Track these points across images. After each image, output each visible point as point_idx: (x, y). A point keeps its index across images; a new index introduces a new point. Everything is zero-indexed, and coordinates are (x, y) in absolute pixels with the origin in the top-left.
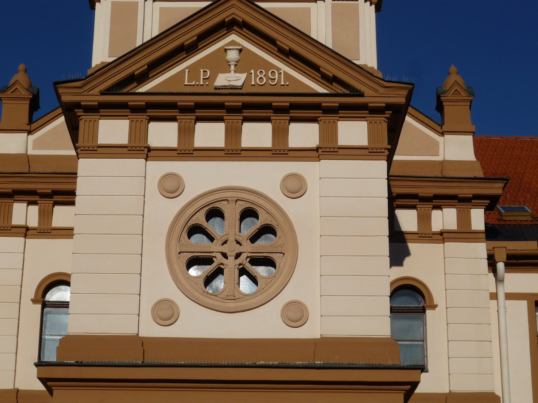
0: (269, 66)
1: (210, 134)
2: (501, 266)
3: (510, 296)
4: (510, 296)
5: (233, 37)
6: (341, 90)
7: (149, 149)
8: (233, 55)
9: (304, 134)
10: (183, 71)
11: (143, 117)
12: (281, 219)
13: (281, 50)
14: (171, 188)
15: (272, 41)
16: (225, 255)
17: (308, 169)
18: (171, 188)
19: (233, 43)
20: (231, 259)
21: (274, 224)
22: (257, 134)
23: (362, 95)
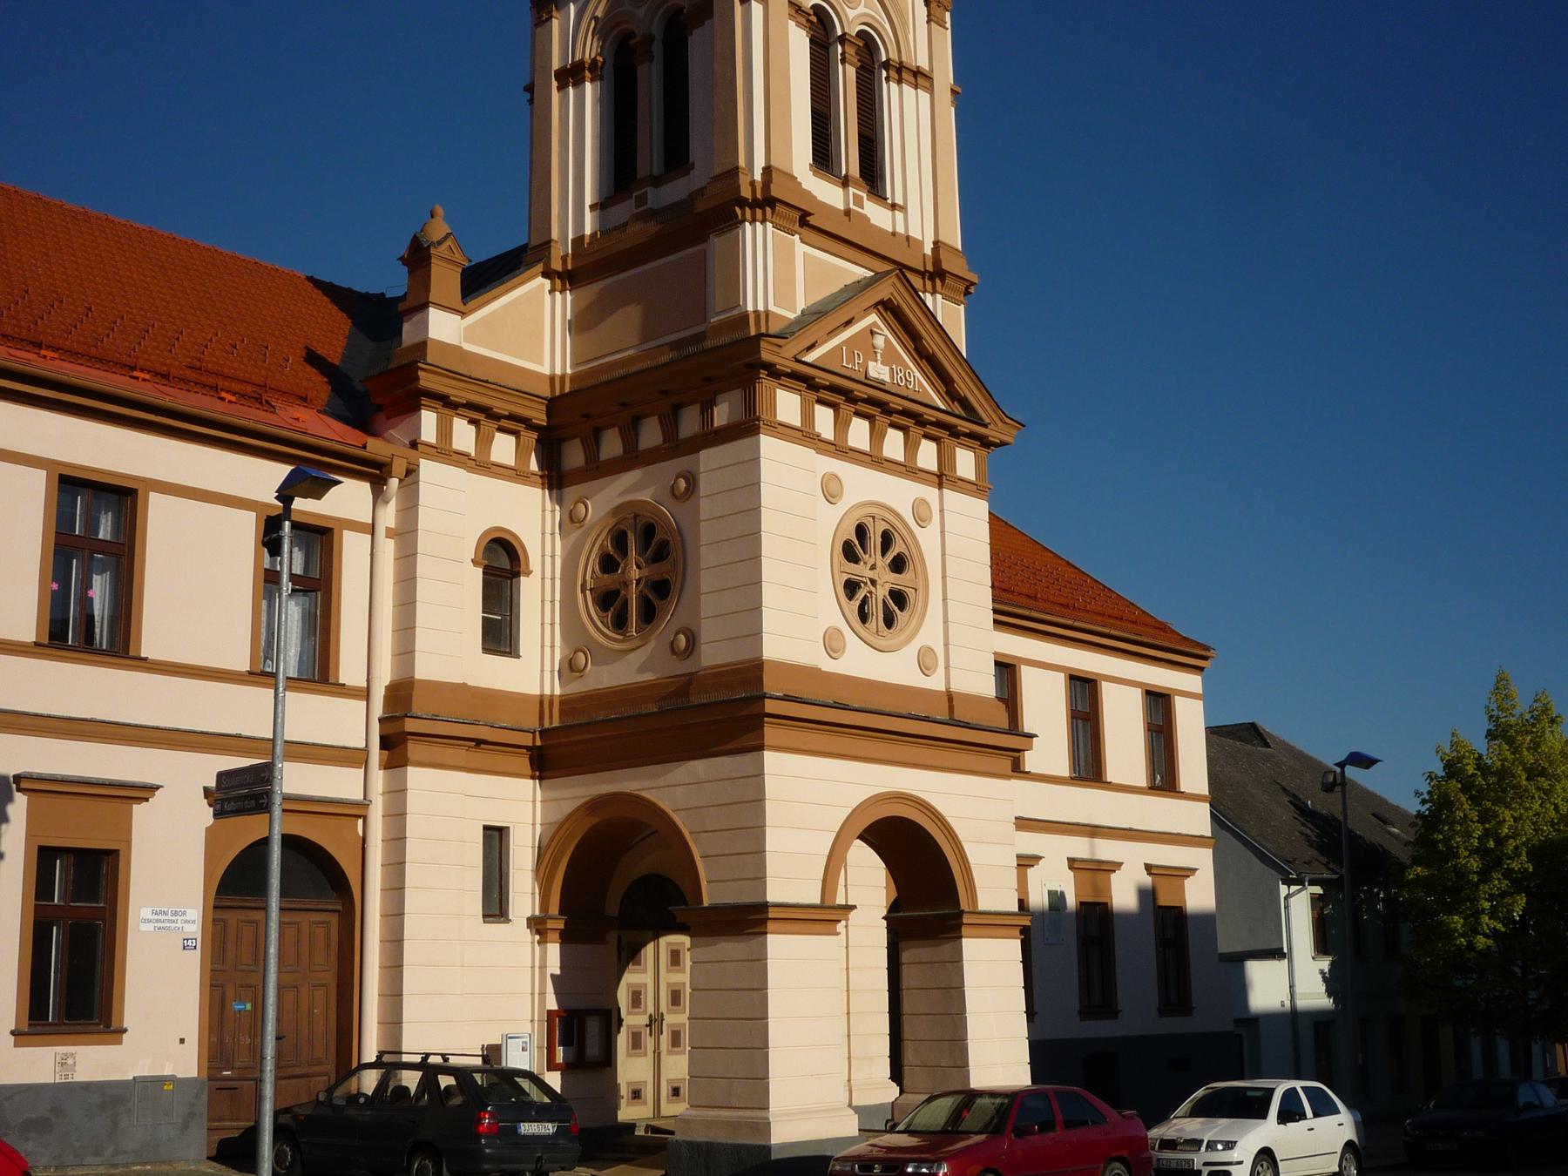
10: (839, 347)
16: (873, 582)
18: (831, 490)
23: (986, 426)
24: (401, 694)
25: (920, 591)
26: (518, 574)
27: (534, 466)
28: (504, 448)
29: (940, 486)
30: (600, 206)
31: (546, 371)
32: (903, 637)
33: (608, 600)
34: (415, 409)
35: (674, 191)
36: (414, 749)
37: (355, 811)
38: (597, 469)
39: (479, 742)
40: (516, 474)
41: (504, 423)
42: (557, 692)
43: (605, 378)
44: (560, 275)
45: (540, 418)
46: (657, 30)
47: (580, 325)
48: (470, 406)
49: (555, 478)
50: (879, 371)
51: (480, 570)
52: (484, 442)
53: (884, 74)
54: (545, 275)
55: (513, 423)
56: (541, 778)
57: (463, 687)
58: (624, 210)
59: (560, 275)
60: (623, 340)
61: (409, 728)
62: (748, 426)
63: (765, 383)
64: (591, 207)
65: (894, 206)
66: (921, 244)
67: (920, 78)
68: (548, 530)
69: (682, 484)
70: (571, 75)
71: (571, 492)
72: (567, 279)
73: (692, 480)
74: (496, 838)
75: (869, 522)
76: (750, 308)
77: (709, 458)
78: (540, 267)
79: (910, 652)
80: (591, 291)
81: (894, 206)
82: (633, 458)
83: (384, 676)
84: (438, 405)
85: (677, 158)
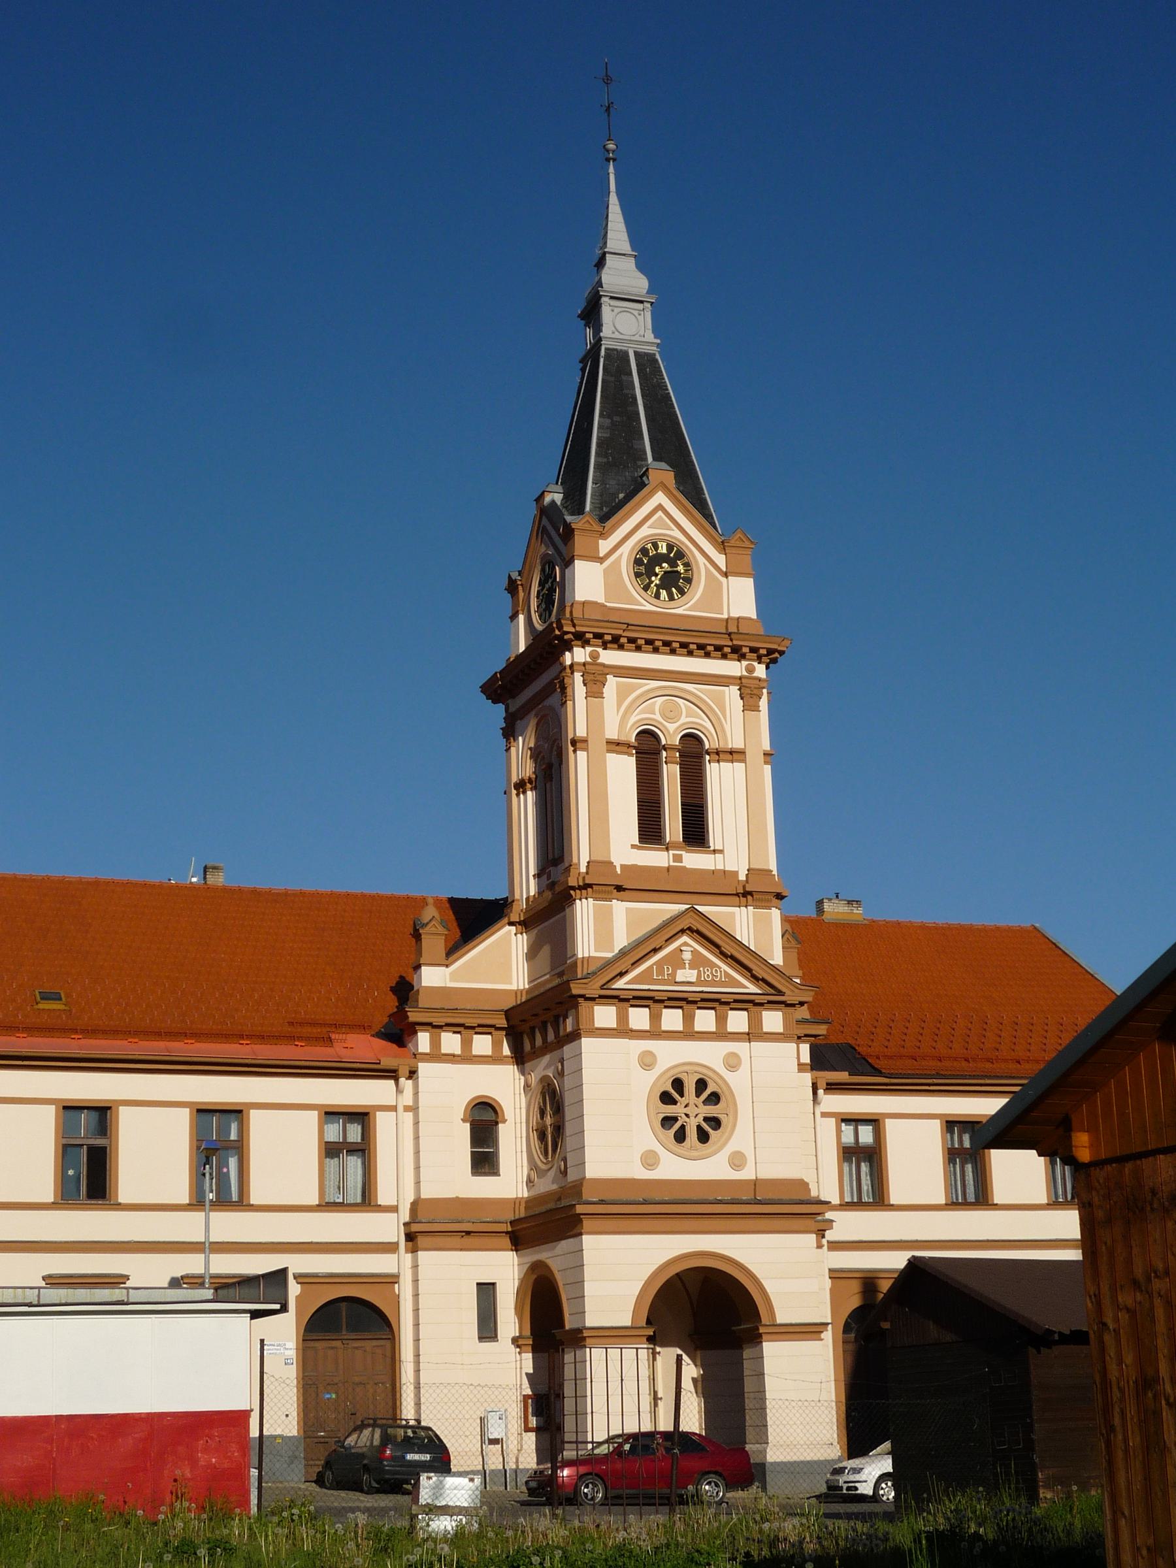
0: (713, 965)
1: (672, 1019)
2: (821, 1092)
3: (824, 1115)
4: (824, 1115)
5: (685, 938)
6: (773, 991)
7: (632, 1031)
8: (687, 956)
9: (738, 1021)
10: (651, 967)
11: (626, 1004)
12: (724, 1088)
13: (722, 953)
14: (647, 1061)
15: (718, 946)
16: (687, 1115)
17: (741, 1048)
18: (647, 1061)
19: (686, 944)
20: (692, 1118)
21: (719, 1091)
22: (705, 1020)
23: (783, 994)
24: (415, 1206)
25: (731, 1117)
26: (497, 1123)
27: (506, 1051)
28: (482, 1044)
30: (538, 876)
31: (514, 987)
32: (715, 1148)
33: (542, 1136)
34: (415, 1033)
36: (421, 1240)
37: (392, 1280)
38: (537, 1053)
39: (468, 1233)
40: (494, 1059)
41: (478, 1030)
42: (526, 1195)
43: (542, 990)
44: (520, 923)
45: (503, 1023)
48: (447, 1025)
49: (520, 1058)
50: (686, 975)
51: (468, 1125)
52: (467, 1044)
53: (708, 757)
54: (511, 924)
55: (484, 1029)
56: (517, 1250)
57: (457, 1200)
59: (520, 923)
61: (427, 1227)
63: (584, 1005)
65: (714, 851)
66: (736, 873)
67: (735, 755)
68: (517, 1092)
70: (521, 786)
71: (528, 1065)
74: (486, 1290)
75: (684, 1077)
76: (580, 956)
78: (506, 920)
79: (722, 1157)
80: (535, 931)
81: (714, 851)
83: (411, 1198)
84: (429, 1028)
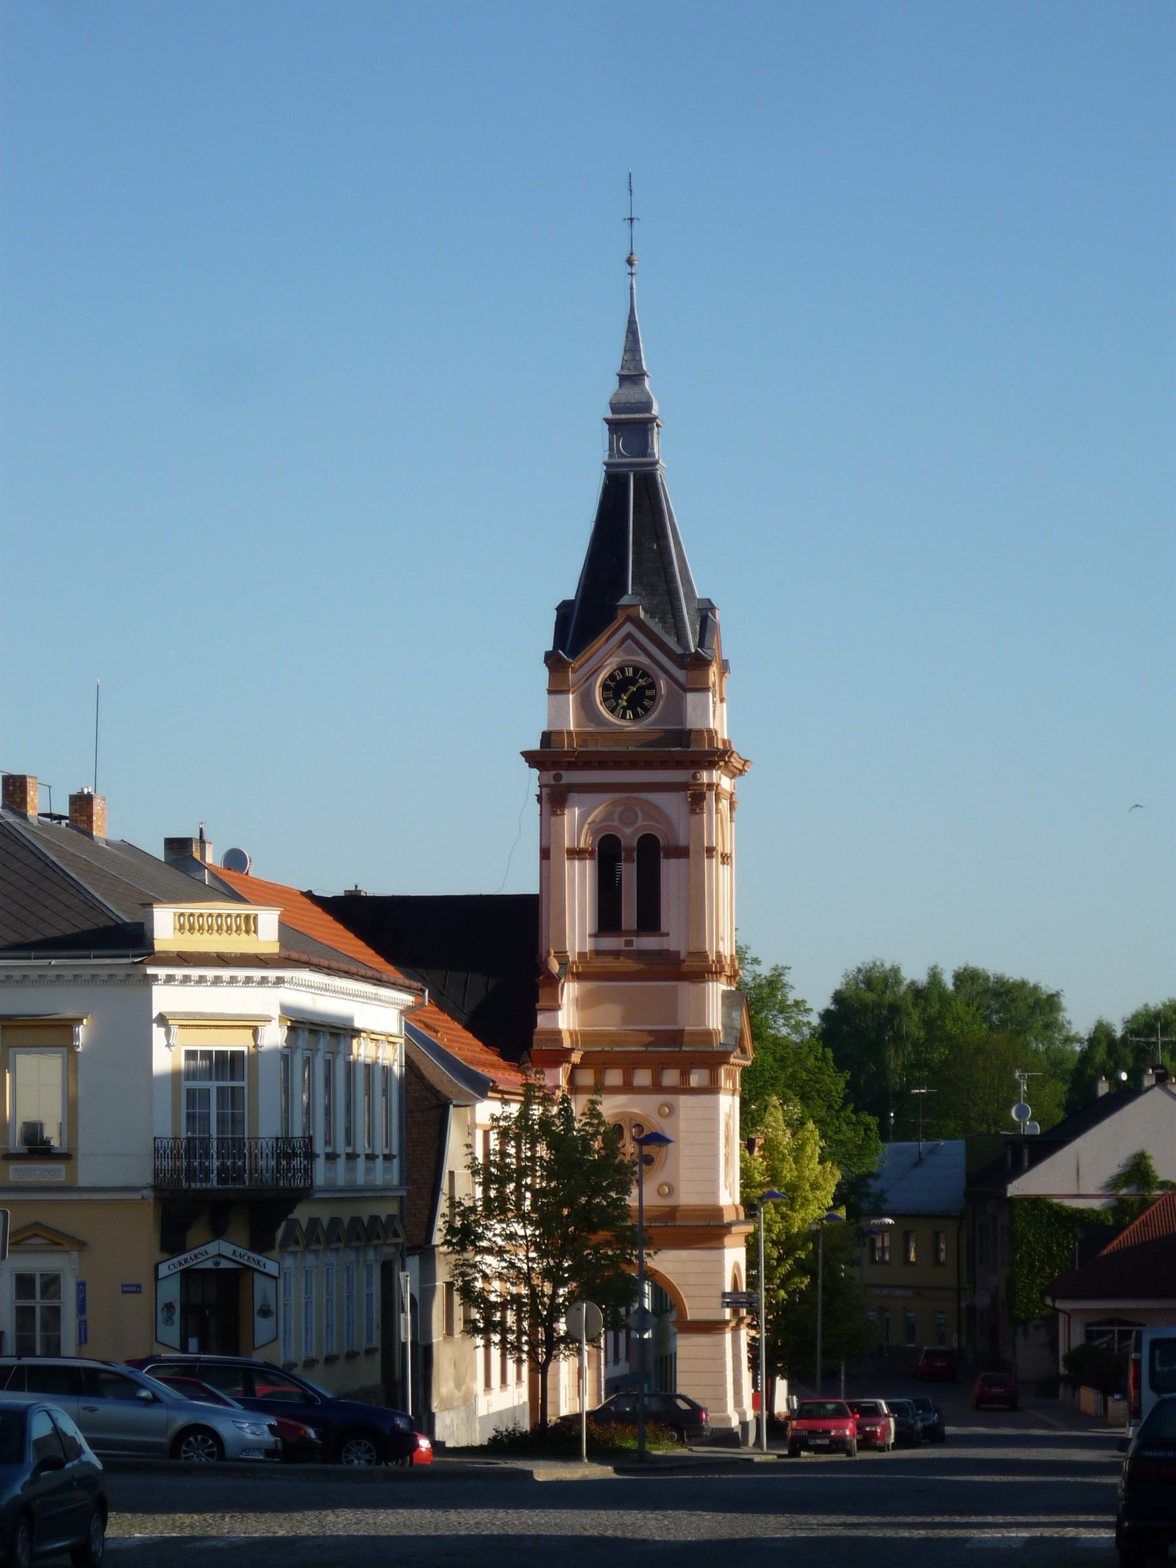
29: (733, 1095)
35: (648, 943)
44: (573, 973)
46: (635, 843)
47: (583, 1003)
58: (611, 943)
60: (609, 1019)
62: (713, 1089)
64: (590, 936)
69: (667, 1110)
70: (575, 854)
72: (578, 977)
73: (672, 1110)
77: (684, 1101)
80: (590, 985)
82: (628, 1087)
85: (650, 921)
